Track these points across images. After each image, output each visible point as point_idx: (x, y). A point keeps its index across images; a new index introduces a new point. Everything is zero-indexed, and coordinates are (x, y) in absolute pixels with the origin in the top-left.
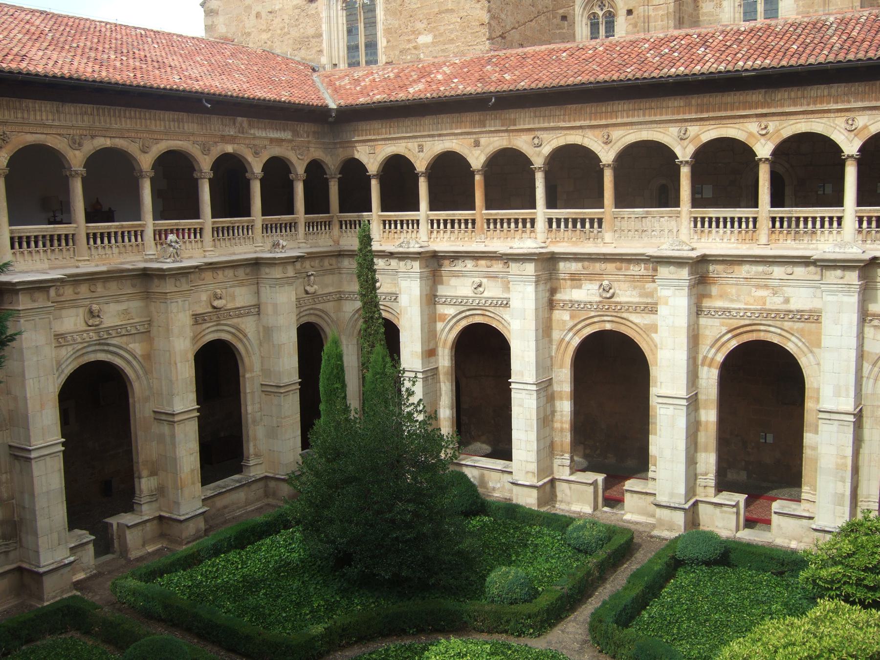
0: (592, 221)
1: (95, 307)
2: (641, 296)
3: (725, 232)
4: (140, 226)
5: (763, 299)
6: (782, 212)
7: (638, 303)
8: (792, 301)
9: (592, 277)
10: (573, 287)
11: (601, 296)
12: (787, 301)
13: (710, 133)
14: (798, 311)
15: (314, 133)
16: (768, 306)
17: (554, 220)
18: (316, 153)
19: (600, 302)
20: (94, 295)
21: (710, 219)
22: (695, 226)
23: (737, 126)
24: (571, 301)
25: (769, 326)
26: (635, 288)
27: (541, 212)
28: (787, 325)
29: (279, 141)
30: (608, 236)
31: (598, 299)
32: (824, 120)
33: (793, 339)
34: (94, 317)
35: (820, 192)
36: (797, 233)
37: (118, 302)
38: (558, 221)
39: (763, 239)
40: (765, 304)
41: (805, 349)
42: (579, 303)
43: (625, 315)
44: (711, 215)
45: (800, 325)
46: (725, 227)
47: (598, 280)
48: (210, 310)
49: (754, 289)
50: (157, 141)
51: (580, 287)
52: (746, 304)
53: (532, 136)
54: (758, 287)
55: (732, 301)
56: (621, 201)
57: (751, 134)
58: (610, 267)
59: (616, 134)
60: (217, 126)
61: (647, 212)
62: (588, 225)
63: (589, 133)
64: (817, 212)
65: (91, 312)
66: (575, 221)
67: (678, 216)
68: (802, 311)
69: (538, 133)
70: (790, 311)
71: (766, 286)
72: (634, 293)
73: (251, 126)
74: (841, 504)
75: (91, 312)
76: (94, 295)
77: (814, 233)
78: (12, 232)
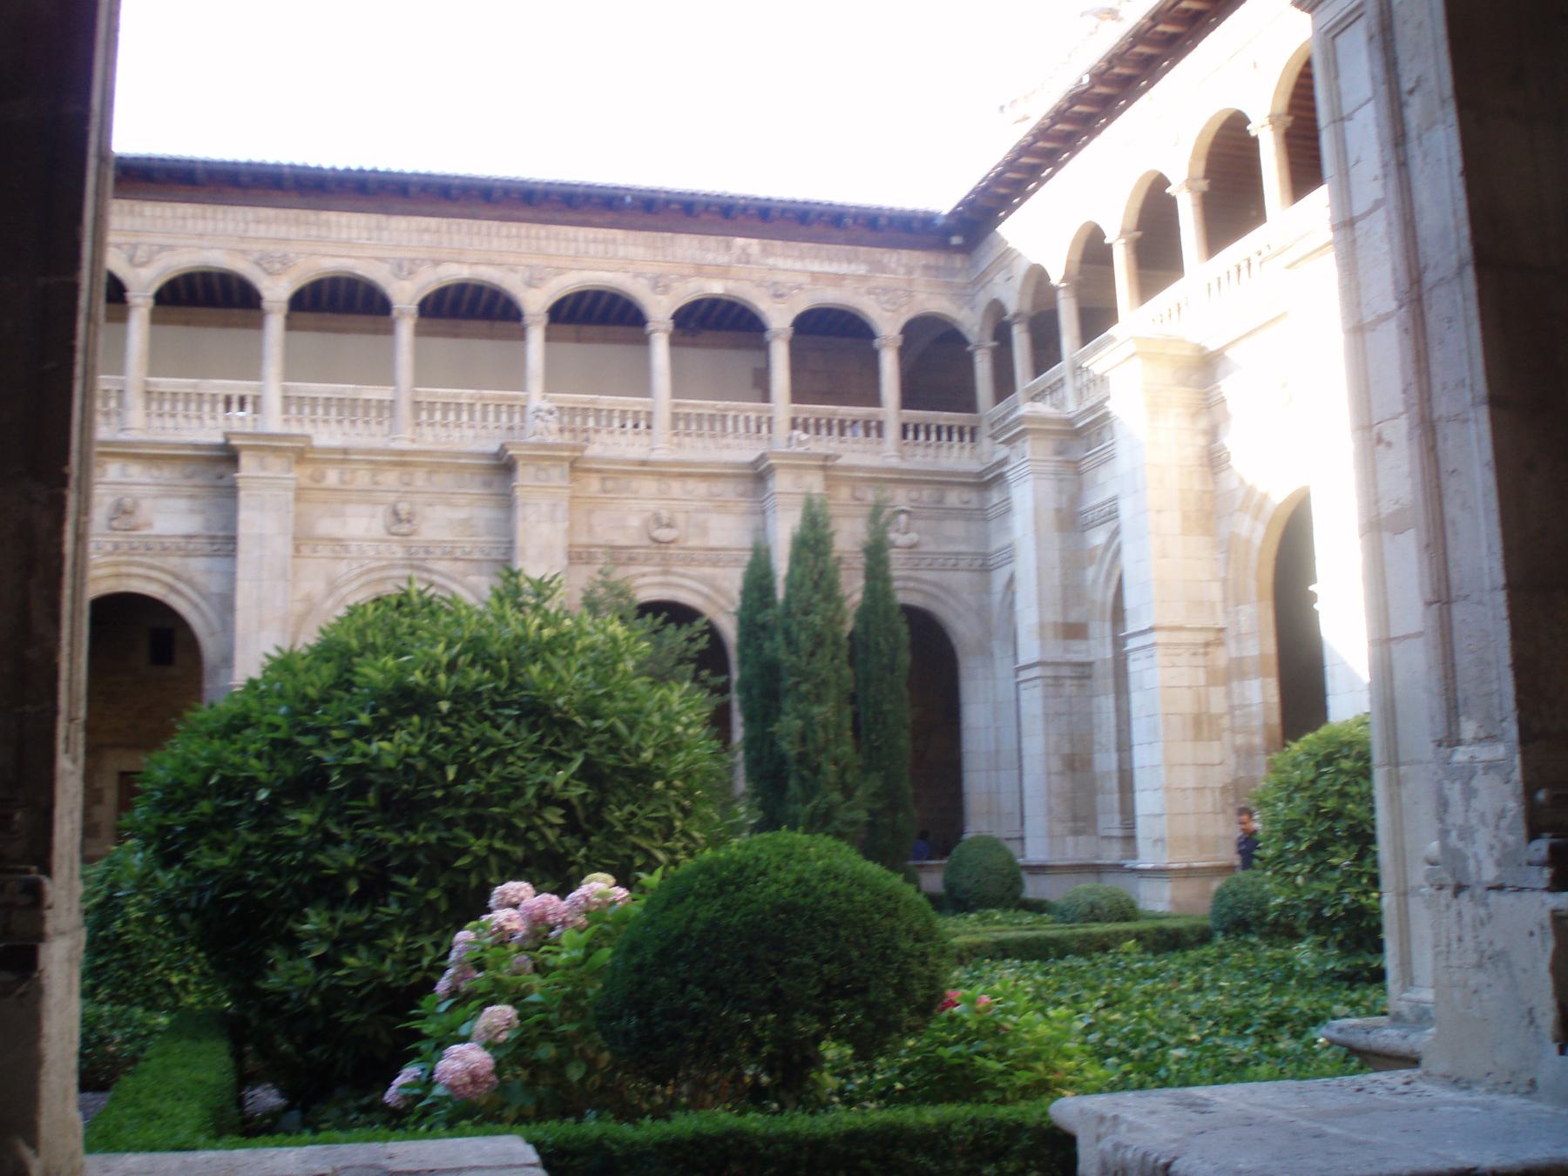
1: (404, 508)
4: (517, 398)
15: (927, 268)
18: (932, 300)
20: (408, 489)
29: (838, 279)
34: (400, 521)
37: (450, 505)
48: (647, 542)
50: (560, 271)
60: (687, 247)
65: (396, 513)
73: (765, 252)
75: (396, 513)
76: (408, 489)
78: (285, 389)
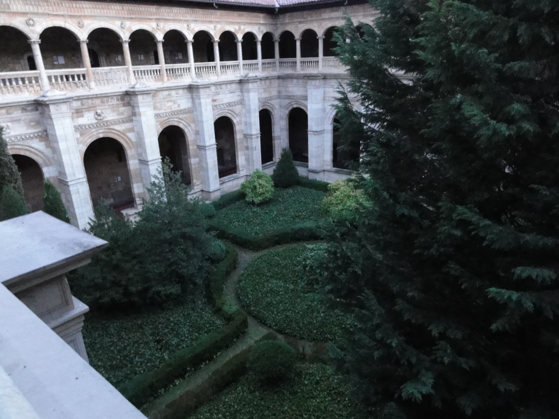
0: (78, 76)
2: (118, 115)
3: (149, 78)
5: (170, 106)
6: (184, 66)
7: (119, 119)
8: (181, 106)
9: (89, 109)
10: (78, 117)
11: (96, 119)
12: (179, 106)
13: (136, 26)
14: (184, 109)
16: (173, 109)
17: (53, 77)
19: (97, 123)
21: (141, 71)
22: (135, 75)
23: (147, 23)
24: (79, 126)
25: (174, 118)
26: (114, 111)
27: (42, 70)
28: (181, 116)
30: (93, 84)
31: (96, 121)
32: (180, 24)
33: (183, 122)
35: (117, 60)
36: (176, 75)
38: (56, 77)
39: (166, 78)
40: (171, 109)
41: (187, 125)
42: (85, 126)
43: (112, 127)
44: (141, 69)
45: (185, 115)
46: (151, 74)
47: (94, 110)
49: (166, 103)
51: (83, 116)
52: (165, 110)
53: (26, 19)
54: (168, 102)
55: (159, 110)
56: (95, 63)
57: (153, 28)
58: (97, 102)
59: (86, 22)
61: (111, 69)
62: (76, 79)
63: (69, 20)
64: (181, 66)
66: (67, 77)
67: (127, 70)
68: (186, 109)
69: (31, 16)
70: (181, 110)
71: (171, 101)
72: (114, 114)
74: (216, 179)
77: (182, 75)
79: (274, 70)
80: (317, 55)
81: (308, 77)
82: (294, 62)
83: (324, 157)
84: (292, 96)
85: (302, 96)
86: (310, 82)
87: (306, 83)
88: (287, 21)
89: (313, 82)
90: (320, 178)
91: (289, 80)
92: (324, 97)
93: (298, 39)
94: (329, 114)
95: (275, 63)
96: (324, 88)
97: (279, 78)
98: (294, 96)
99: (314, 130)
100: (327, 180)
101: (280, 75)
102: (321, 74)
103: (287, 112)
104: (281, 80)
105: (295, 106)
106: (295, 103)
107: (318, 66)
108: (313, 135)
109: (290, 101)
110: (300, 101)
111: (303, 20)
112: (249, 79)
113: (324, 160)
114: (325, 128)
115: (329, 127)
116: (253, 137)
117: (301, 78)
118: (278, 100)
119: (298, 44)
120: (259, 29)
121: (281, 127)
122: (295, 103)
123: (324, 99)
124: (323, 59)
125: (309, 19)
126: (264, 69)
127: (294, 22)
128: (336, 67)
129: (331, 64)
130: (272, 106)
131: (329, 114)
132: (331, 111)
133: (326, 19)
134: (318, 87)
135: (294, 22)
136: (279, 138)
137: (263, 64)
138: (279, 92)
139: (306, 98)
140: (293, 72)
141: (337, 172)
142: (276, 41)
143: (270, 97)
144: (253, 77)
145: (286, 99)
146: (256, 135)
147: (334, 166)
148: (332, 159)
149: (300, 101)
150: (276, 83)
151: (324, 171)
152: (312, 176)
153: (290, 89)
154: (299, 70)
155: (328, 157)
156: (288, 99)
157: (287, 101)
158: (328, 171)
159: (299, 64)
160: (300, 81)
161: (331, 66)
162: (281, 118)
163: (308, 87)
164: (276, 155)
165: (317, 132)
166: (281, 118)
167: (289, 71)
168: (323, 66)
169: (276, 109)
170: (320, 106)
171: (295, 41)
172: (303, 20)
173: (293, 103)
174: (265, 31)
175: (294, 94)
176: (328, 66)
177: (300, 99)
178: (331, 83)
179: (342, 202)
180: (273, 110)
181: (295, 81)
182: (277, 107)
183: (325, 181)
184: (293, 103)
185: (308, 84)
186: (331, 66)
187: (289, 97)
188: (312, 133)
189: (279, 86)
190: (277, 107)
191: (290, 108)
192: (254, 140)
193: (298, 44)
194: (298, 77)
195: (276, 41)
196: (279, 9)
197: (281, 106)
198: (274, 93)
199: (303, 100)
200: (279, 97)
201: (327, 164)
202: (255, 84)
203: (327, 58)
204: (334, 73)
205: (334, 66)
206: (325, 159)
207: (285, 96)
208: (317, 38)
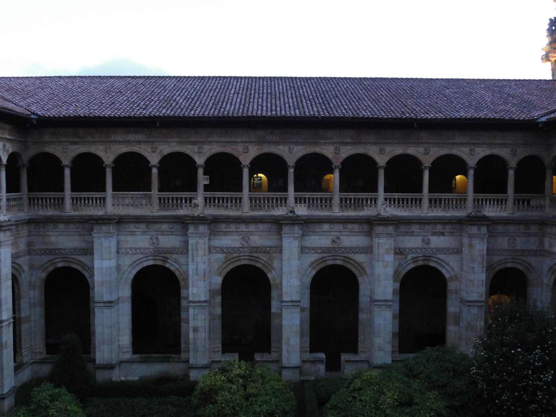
79: (20, 210)
80: (103, 189)
81: (96, 220)
82: (58, 199)
83: (119, 340)
84: (56, 249)
85: (75, 249)
86: (96, 228)
87: (92, 229)
88: (47, 138)
89: (104, 228)
90: (118, 376)
91: (51, 226)
92: (118, 249)
93: (67, 166)
94: (127, 273)
95: (21, 199)
96: (118, 235)
97: (30, 222)
98: (61, 249)
99: (105, 299)
100: (125, 376)
101: (33, 217)
102: (115, 215)
103: (44, 275)
104: (33, 225)
105: (60, 265)
106: (61, 260)
107: (104, 205)
108: (104, 308)
109: (52, 257)
110: (72, 256)
111: (77, 140)
112: (4, 224)
113: (119, 346)
114: (120, 295)
115: (126, 292)
116: (5, 324)
117: (73, 223)
118: (27, 257)
119: (67, 172)
120: (4, 146)
121: (32, 301)
122: (61, 260)
123: (118, 252)
124: (113, 194)
125: (89, 139)
126: (9, 208)
127: (60, 142)
128: (137, 206)
129: (127, 201)
130: (18, 267)
131: (127, 273)
132: (130, 268)
133: (119, 142)
134: (109, 235)
135: (60, 142)
136: (28, 319)
137: (8, 200)
138: (29, 244)
139: (89, 251)
140: (57, 213)
141: (145, 361)
142: (24, 166)
143: (18, 253)
144: (5, 221)
145: (42, 254)
146: (8, 320)
147: (134, 352)
148: (132, 342)
149: (72, 256)
150: (24, 231)
151: (121, 362)
152: (101, 376)
153: (53, 239)
154: (69, 210)
155: (126, 339)
156: (47, 254)
157: (46, 258)
158: (128, 362)
159: (68, 202)
160: (72, 226)
161: (127, 205)
162: (32, 286)
163: (94, 235)
164: (23, 350)
165: (112, 302)
166: (32, 286)
167: (50, 212)
168: (113, 205)
169: (23, 271)
170: (113, 263)
171: (62, 169)
172: (77, 140)
173: (56, 261)
174: (11, 151)
175: (60, 247)
176: (122, 205)
177: (72, 254)
178: (129, 228)
179: (241, 409)
180: (20, 274)
181: (61, 226)
182: (26, 268)
183: (123, 379)
184: (56, 261)
185: (95, 231)
186: (127, 205)
187: (51, 252)
188: (102, 305)
189: (29, 236)
190: (26, 268)
191: (51, 268)
192: (4, 330)
193: (67, 172)
194: (69, 221)
195: (24, 166)
196: (37, 120)
197: (31, 267)
198: (22, 246)
199: (77, 255)
200: (29, 252)
201: (125, 350)
202: (8, 233)
203: (121, 194)
204: (134, 214)
205: (132, 205)
206: (121, 343)
207: (41, 250)
208: (104, 166)
